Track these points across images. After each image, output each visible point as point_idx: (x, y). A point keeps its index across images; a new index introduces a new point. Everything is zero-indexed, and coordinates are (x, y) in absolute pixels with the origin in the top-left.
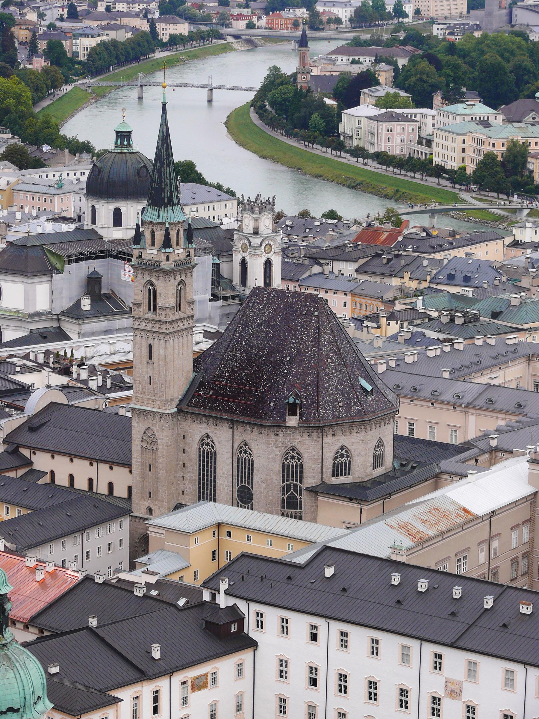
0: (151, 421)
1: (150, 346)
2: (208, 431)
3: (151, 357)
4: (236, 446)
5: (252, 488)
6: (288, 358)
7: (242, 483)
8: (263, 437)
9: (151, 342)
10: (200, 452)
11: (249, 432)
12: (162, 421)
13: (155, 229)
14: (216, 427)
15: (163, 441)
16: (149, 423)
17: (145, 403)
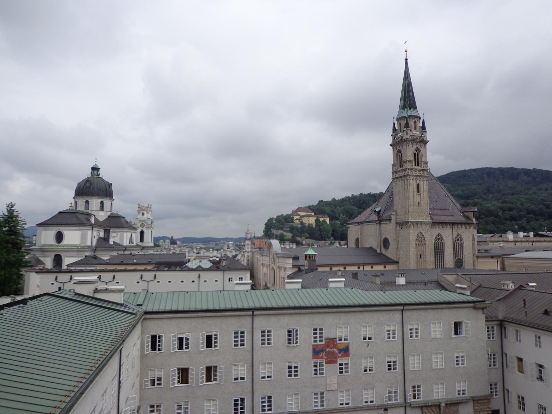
0: (421, 228)
1: (418, 185)
2: (439, 232)
3: (418, 191)
4: (454, 238)
5: (463, 258)
6: (446, 196)
7: (457, 257)
8: (467, 230)
9: (419, 182)
10: (435, 244)
11: (460, 228)
12: (427, 227)
13: (416, 120)
14: (443, 229)
15: (429, 238)
16: (420, 229)
17: (417, 218)
